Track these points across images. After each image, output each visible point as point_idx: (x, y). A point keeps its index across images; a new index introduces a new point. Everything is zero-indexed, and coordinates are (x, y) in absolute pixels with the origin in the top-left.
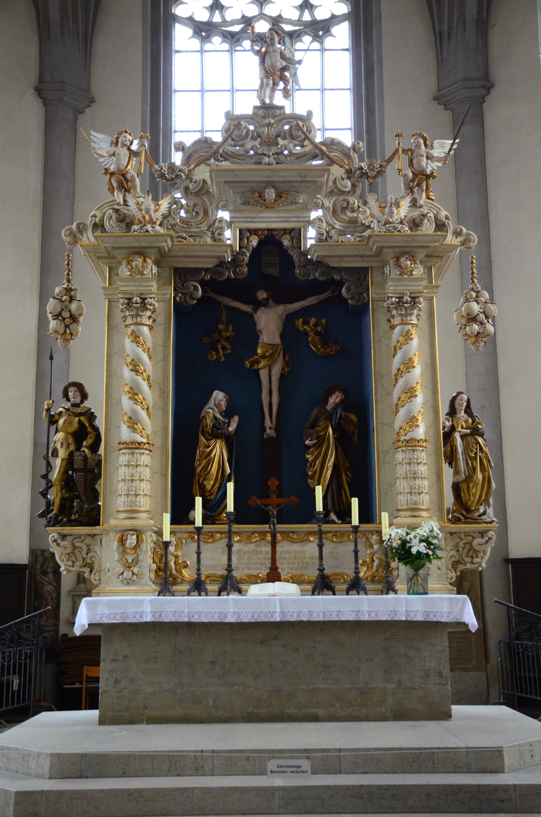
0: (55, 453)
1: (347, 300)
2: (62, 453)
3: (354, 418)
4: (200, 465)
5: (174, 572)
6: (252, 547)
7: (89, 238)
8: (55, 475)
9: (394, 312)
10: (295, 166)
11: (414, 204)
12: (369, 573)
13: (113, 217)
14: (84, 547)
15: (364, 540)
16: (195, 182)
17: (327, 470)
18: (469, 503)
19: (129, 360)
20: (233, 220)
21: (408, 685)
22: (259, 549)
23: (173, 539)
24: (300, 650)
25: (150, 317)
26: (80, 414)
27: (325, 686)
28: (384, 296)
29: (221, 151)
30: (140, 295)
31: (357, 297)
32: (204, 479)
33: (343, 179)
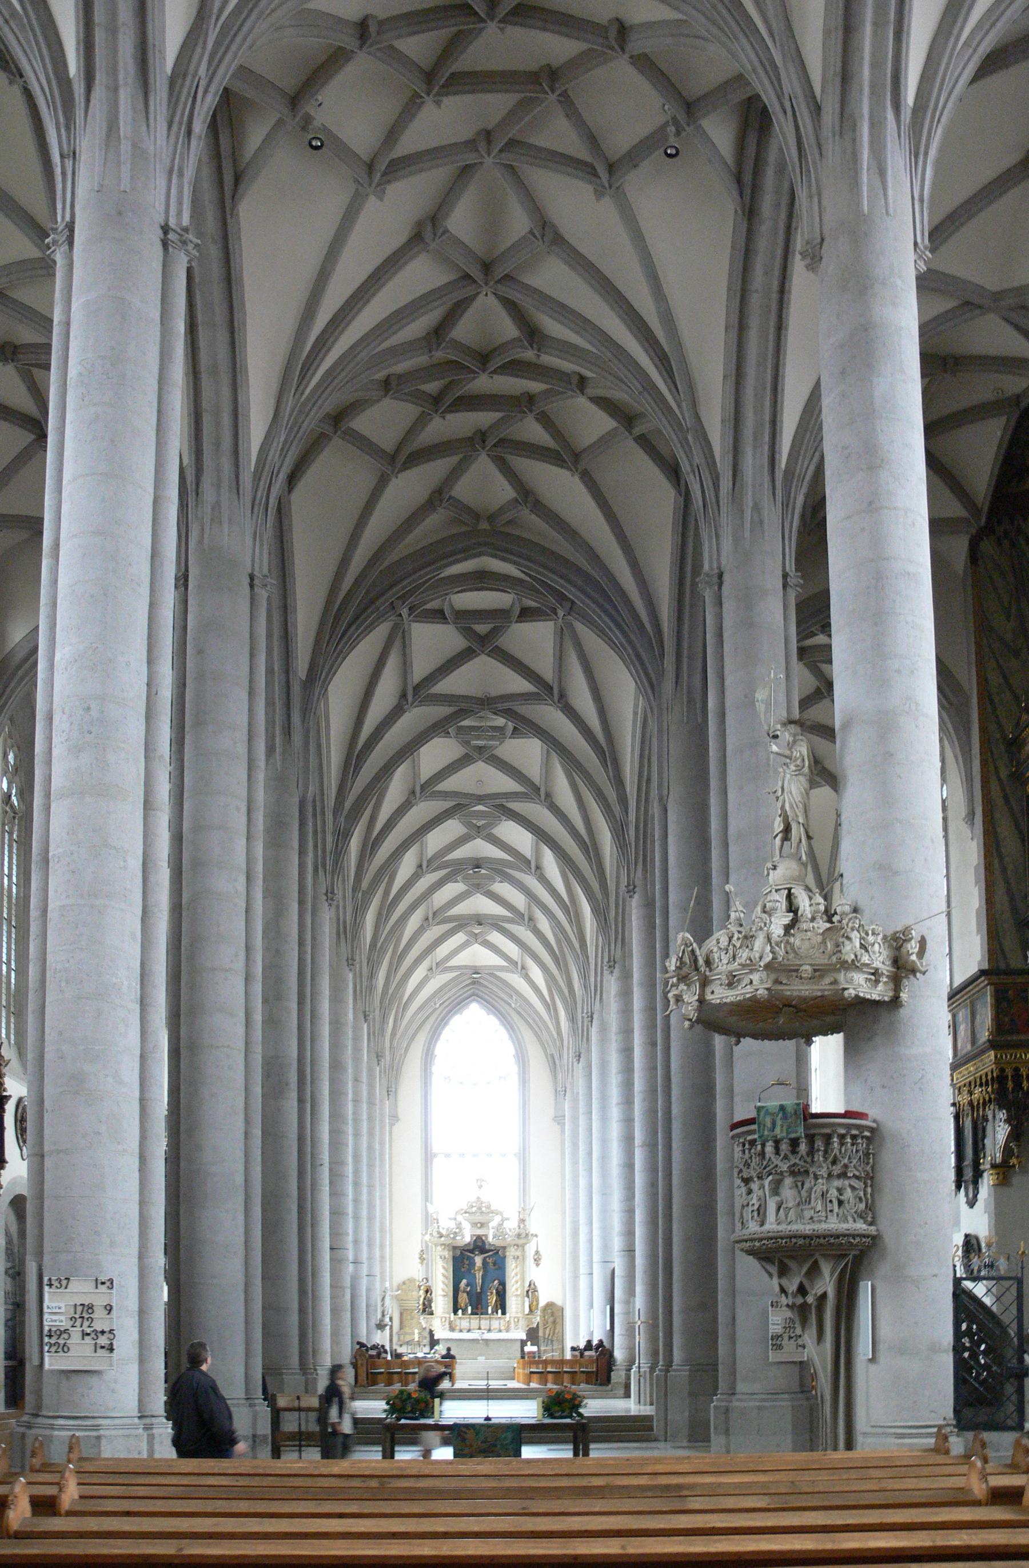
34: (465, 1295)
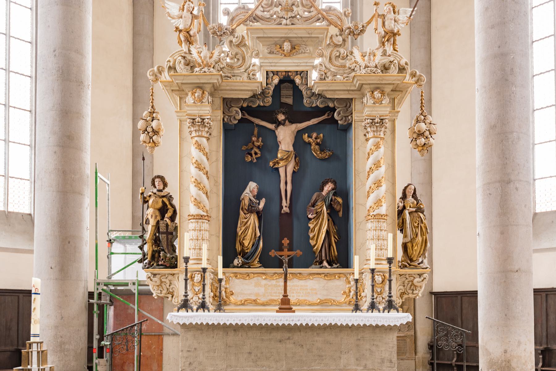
0: (147, 222)
1: (337, 121)
2: (152, 222)
3: (340, 200)
4: (241, 230)
5: (224, 297)
6: (274, 282)
7: (166, 76)
8: (147, 236)
9: (369, 129)
10: (304, 26)
11: (384, 54)
12: (348, 299)
13: (182, 62)
14: (168, 282)
15: (345, 279)
16: (237, 38)
17: (322, 234)
18: (412, 256)
19: (194, 161)
20: (262, 64)
21: (371, 368)
22: (278, 284)
23: (224, 277)
24: (304, 346)
25: (208, 132)
26: (163, 197)
27: (319, 368)
28: (362, 118)
29: (254, 15)
30: (200, 116)
31: (344, 119)
32: (243, 240)
33: (337, 36)
34: (253, 219)
